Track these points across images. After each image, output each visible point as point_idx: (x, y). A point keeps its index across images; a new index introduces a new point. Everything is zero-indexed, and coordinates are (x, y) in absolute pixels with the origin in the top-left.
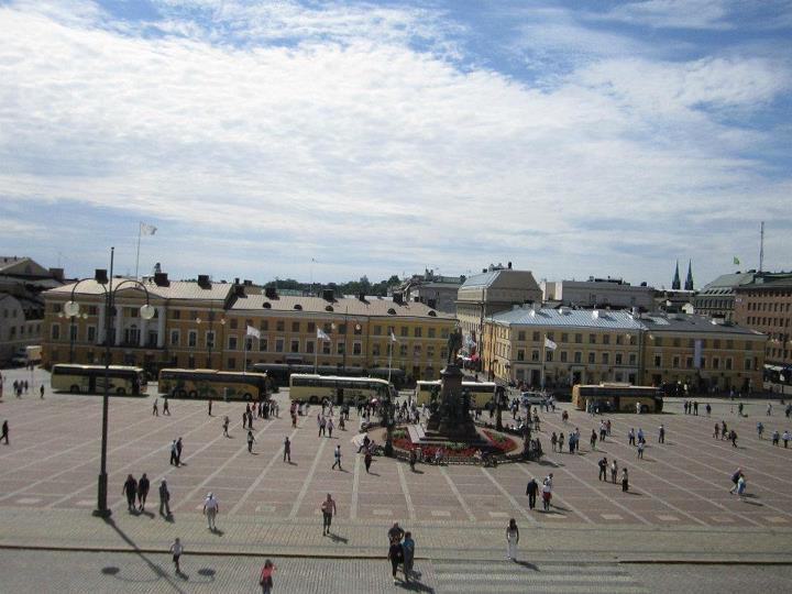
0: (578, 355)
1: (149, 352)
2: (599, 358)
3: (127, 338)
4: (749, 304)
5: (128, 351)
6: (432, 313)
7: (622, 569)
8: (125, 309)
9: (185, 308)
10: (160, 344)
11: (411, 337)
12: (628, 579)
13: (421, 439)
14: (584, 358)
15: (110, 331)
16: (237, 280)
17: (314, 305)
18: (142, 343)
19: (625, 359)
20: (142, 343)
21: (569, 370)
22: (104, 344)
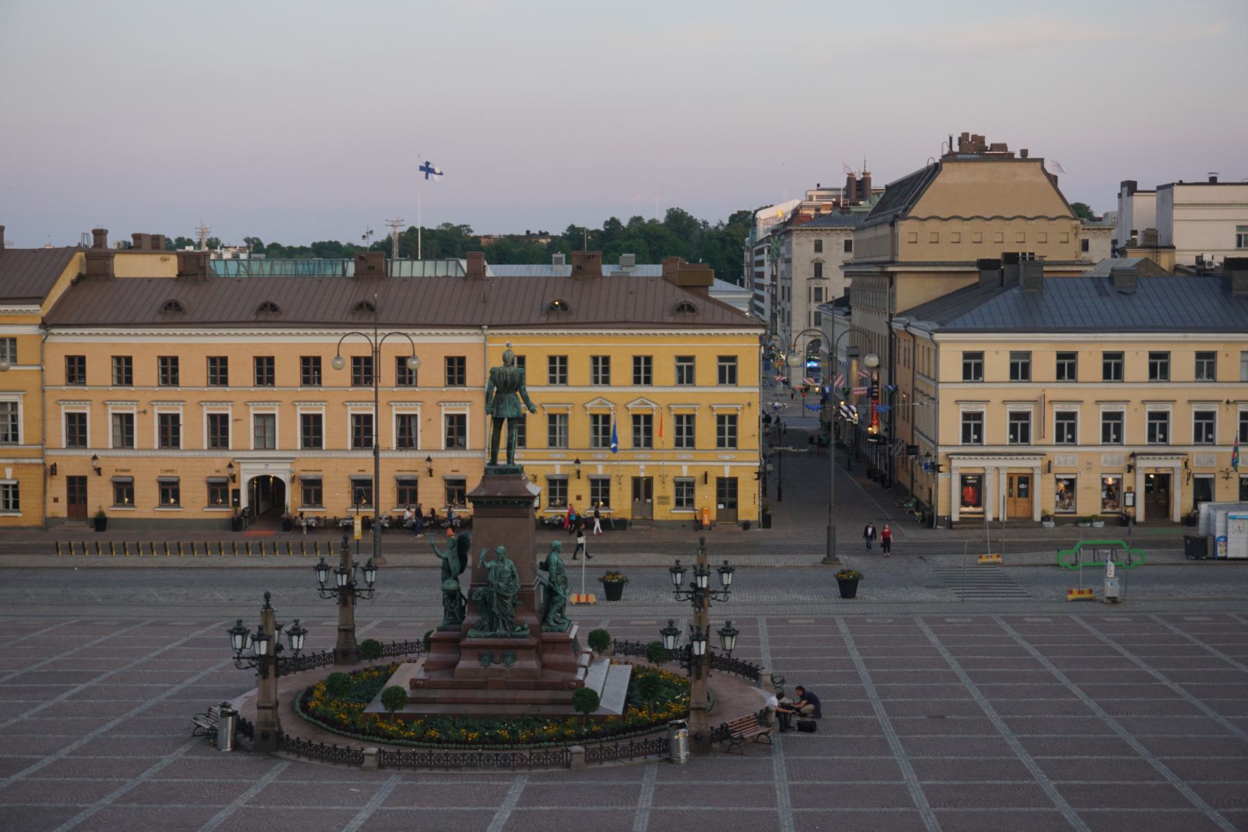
0: (1158, 424)
14: (1181, 428)
16: (100, 234)
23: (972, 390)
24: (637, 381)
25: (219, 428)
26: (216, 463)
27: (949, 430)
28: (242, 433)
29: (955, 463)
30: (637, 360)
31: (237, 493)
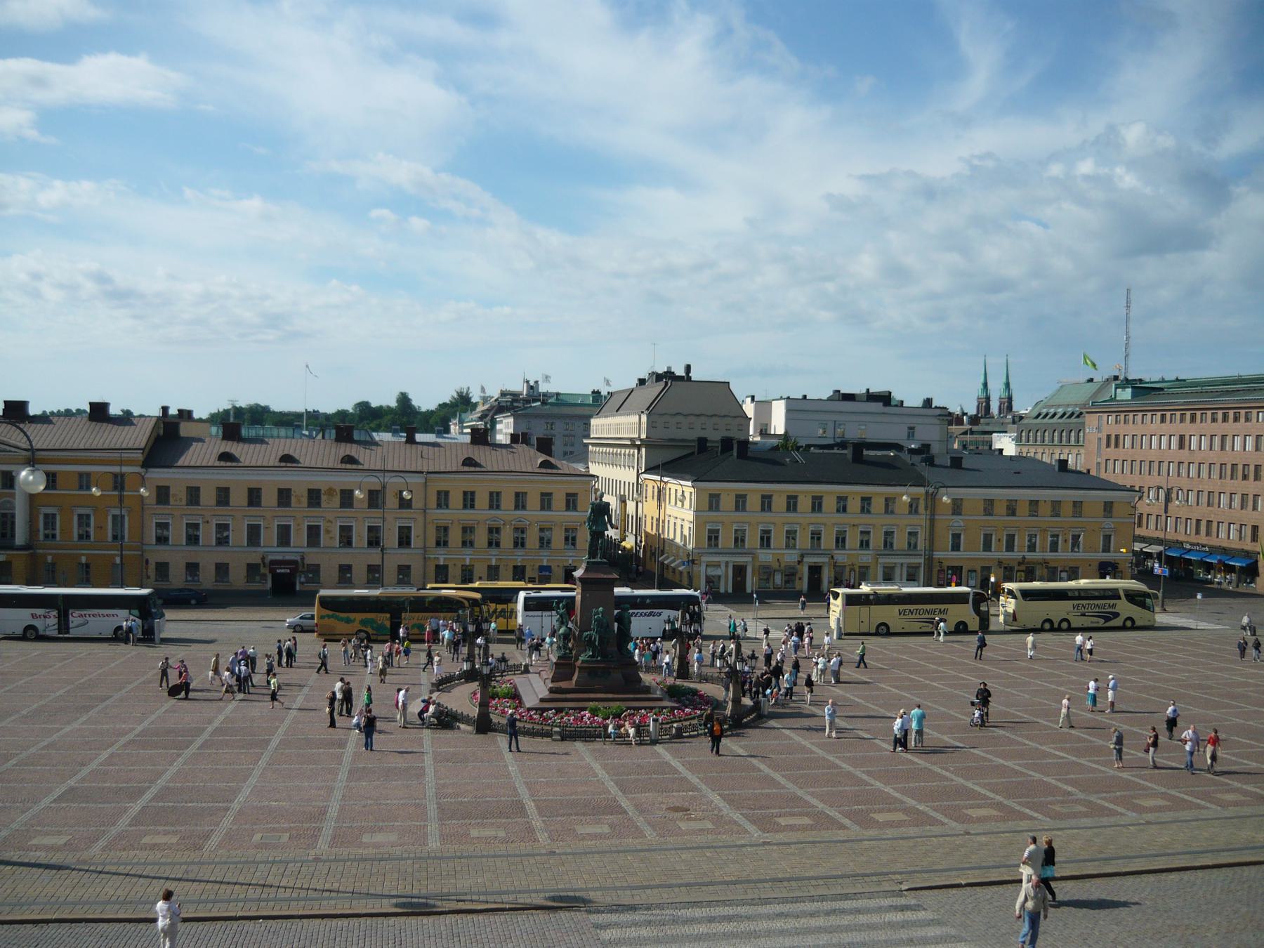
0: (816, 536)
2: (853, 540)
4: (1109, 436)
7: (910, 900)
12: (921, 915)
13: (542, 700)
14: (828, 542)
16: (165, 409)
17: (318, 452)
19: (900, 542)
25: (254, 534)
26: (254, 556)
28: (269, 537)
29: (880, 560)
30: (517, 494)
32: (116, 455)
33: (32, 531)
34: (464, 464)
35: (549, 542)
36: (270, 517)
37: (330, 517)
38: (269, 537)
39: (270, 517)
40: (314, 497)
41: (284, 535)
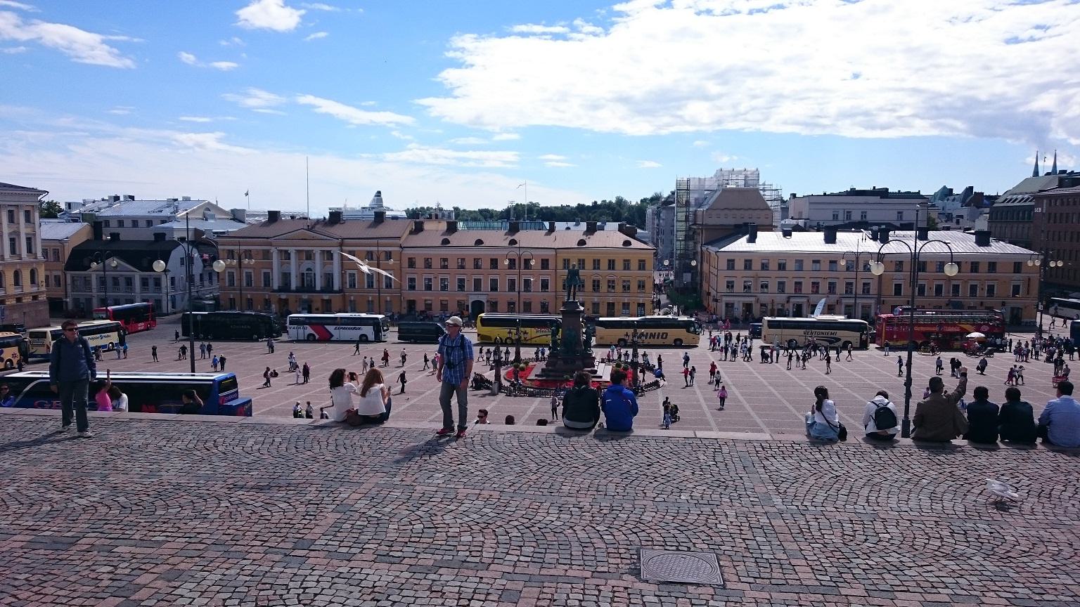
0: (798, 284)
1: (326, 297)
3: (303, 282)
5: (305, 296)
6: (627, 243)
8: (298, 251)
9: (376, 249)
10: (336, 287)
11: (634, 271)
15: (286, 276)
17: (496, 238)
18: (318, 288)
20: (318, 288)
21: (788, 302)
22: (280, 290)
23: (730, 273)
24: (609, 269)
27: (723, 288)
28: (470, 286)
31: (468, 306)
32: (376, 241)
33: (343, 283)
34: (579, 244)
35: (629, 288)
36: (470, 276)
37: (503, 277)
38: (470, 286)
39: (470, 276)
40: (494, 263)
41: (478, 284)
